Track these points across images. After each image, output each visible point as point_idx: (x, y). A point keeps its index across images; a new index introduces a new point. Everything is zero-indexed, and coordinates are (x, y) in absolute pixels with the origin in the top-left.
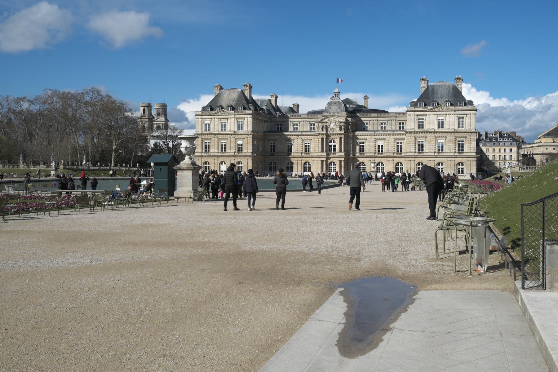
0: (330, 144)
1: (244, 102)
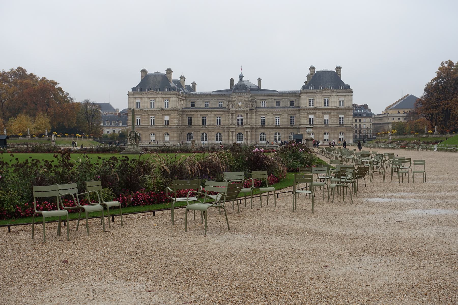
0: (238, 118)
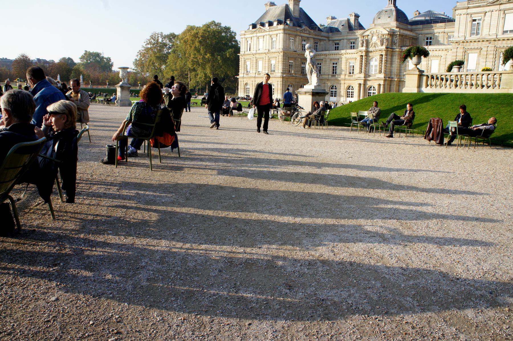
1: (282, 18)
